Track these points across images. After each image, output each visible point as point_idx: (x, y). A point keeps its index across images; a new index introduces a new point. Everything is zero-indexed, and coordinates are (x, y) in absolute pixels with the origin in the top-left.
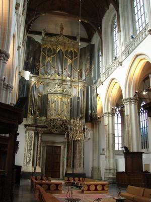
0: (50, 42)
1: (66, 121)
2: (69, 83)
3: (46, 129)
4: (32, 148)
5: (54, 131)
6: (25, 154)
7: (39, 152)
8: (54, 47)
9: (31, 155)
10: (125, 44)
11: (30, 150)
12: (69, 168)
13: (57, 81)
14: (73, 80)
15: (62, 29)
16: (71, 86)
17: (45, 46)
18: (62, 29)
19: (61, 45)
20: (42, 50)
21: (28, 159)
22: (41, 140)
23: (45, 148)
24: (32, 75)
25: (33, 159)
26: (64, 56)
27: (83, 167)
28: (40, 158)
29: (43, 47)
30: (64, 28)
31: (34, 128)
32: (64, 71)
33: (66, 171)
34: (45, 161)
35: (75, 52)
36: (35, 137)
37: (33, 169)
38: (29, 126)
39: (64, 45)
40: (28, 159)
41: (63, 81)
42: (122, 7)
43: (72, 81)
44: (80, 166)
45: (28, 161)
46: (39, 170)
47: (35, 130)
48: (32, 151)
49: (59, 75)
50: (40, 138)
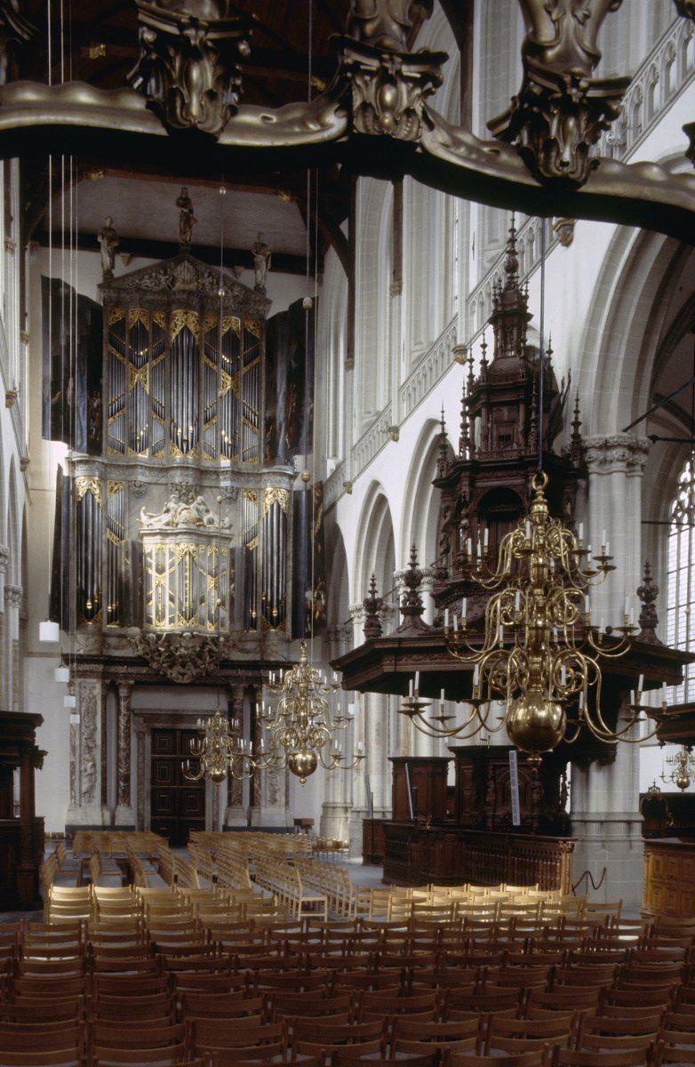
0: (136, 296)
1: (215, 641)
2: (225, 483)
3: (144, 670)
4: (99, 742)
5: (173, 673)
6: (72, 764)
7: (122, 754)
8: (159, 318)
9: (94, 766)
10: (411, 352)
11: (90, 749)
12: (234, 810)
13: (178, 478)
14: (244, 466)
15: (187, 220)
16: (233, 498)
17: (119, 315)
18: (187, 220)
19: (187, 307)
20: (105, 331)
21: (85, 780)
22: (128, 709)
23: (148, 740)
24: (77, 456)
25: (104, 780)
26: (204, 359)
27: (287, 803)
28: (127, 779)
29: (110, 320)
30: (198, 212)
31: (100, 668)
32: (204, 427)
33: (226, 821)
34: (147, 786)
35: (250, 339)
36: (104, 699)
37: (107, 814)
38: (82, 659)
39: (202, 303)
40: (85, 780)
41: (202, 473)
42: (485, 42)
43: (236, 473)
44: (274, 801)
45: (84, 788)
46: (126, 816)
47: (104, 676)
48: (98, 754)
49: (185, 446)
50: (122, 703)
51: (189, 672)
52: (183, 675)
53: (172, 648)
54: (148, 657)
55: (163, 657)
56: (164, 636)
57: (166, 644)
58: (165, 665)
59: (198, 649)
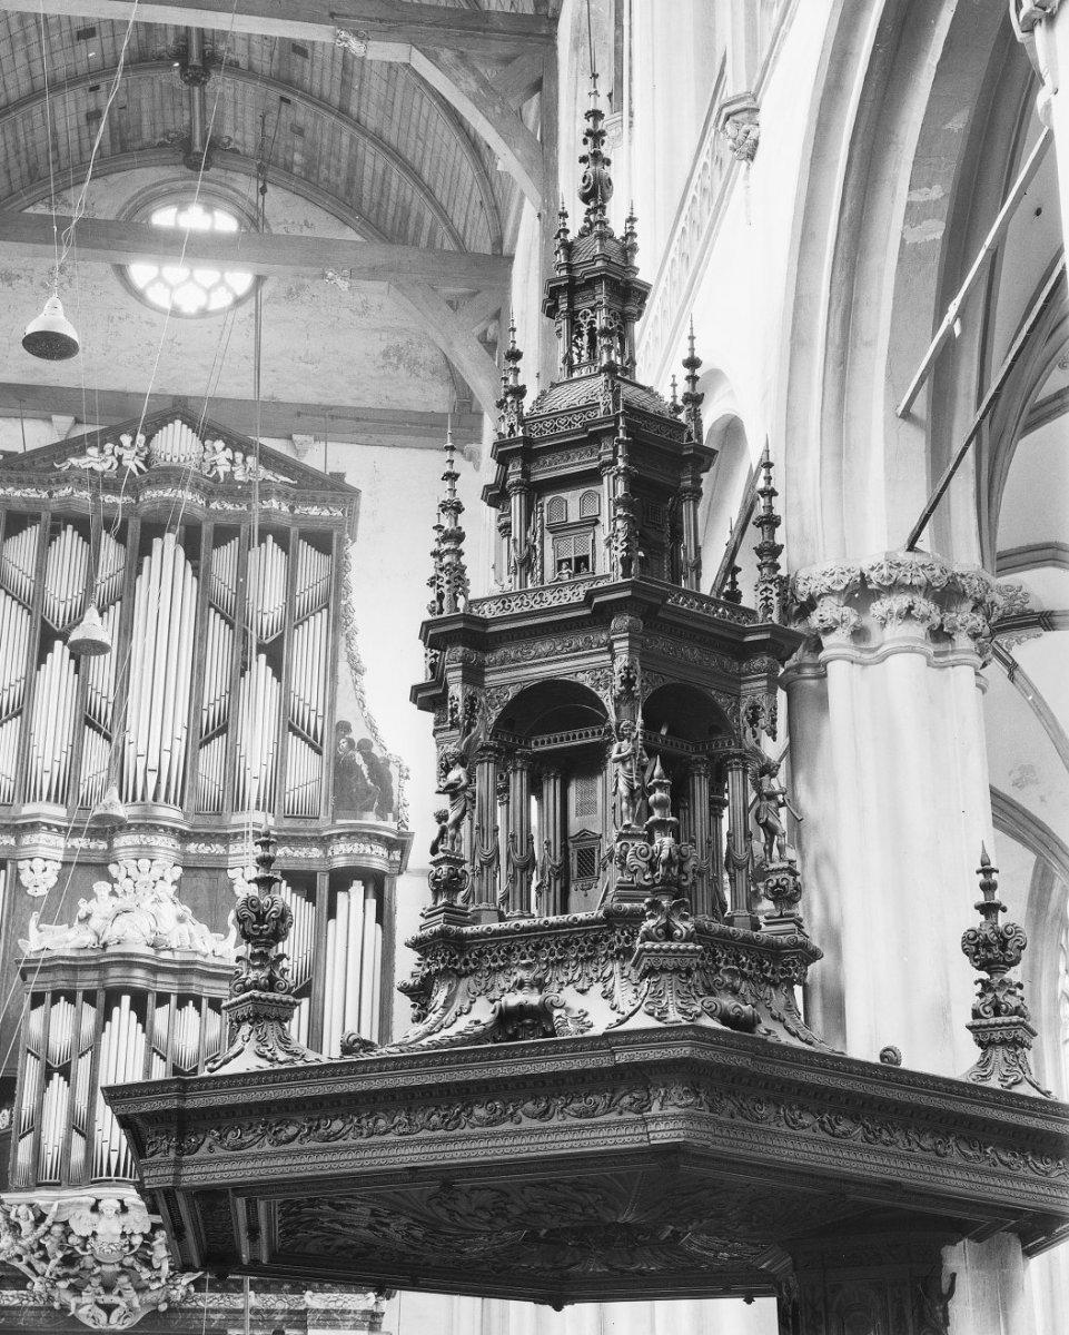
51: (122, 1302)
52: (109, 1309)
53: (72, 1240)
54: (21, 1266)
55: (53, 1262)
56: (55, 1209)
57: (57, 1229)
58: (62, 1285)
59: (137, 1240)
